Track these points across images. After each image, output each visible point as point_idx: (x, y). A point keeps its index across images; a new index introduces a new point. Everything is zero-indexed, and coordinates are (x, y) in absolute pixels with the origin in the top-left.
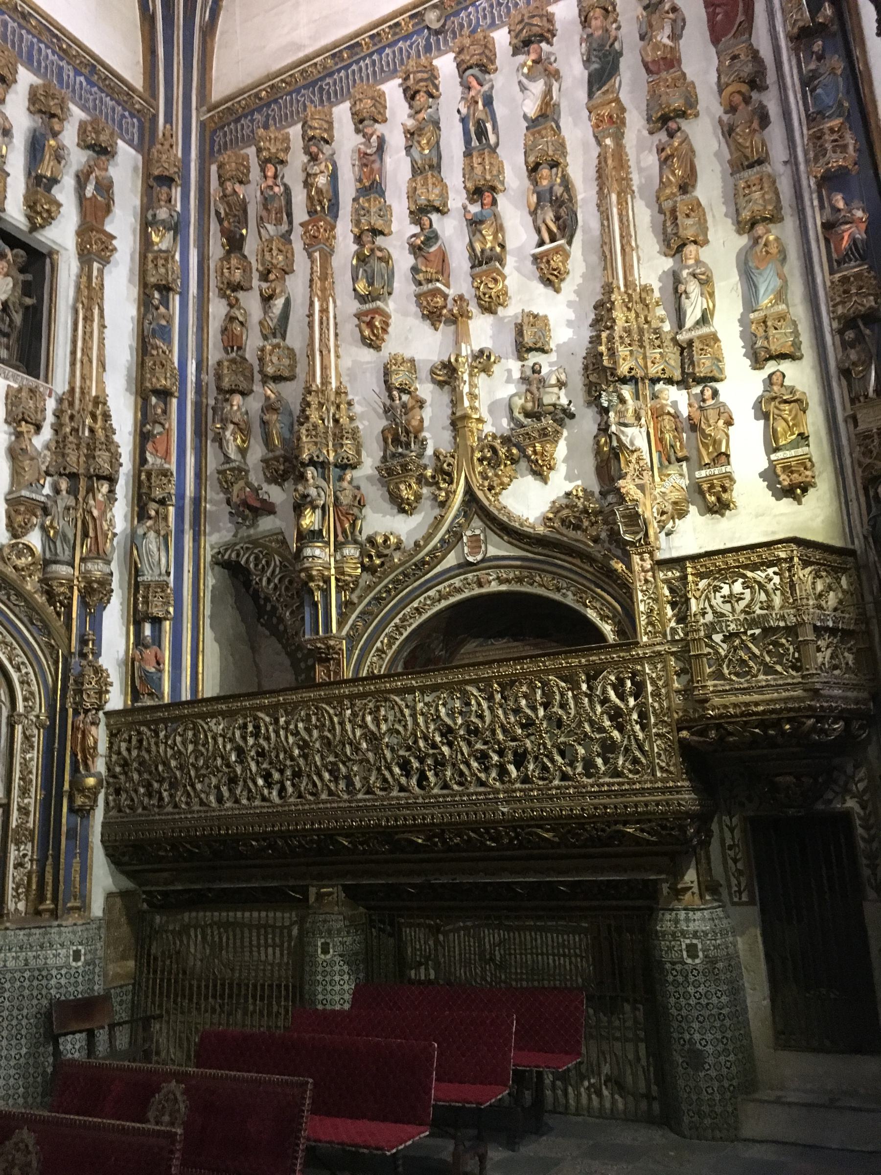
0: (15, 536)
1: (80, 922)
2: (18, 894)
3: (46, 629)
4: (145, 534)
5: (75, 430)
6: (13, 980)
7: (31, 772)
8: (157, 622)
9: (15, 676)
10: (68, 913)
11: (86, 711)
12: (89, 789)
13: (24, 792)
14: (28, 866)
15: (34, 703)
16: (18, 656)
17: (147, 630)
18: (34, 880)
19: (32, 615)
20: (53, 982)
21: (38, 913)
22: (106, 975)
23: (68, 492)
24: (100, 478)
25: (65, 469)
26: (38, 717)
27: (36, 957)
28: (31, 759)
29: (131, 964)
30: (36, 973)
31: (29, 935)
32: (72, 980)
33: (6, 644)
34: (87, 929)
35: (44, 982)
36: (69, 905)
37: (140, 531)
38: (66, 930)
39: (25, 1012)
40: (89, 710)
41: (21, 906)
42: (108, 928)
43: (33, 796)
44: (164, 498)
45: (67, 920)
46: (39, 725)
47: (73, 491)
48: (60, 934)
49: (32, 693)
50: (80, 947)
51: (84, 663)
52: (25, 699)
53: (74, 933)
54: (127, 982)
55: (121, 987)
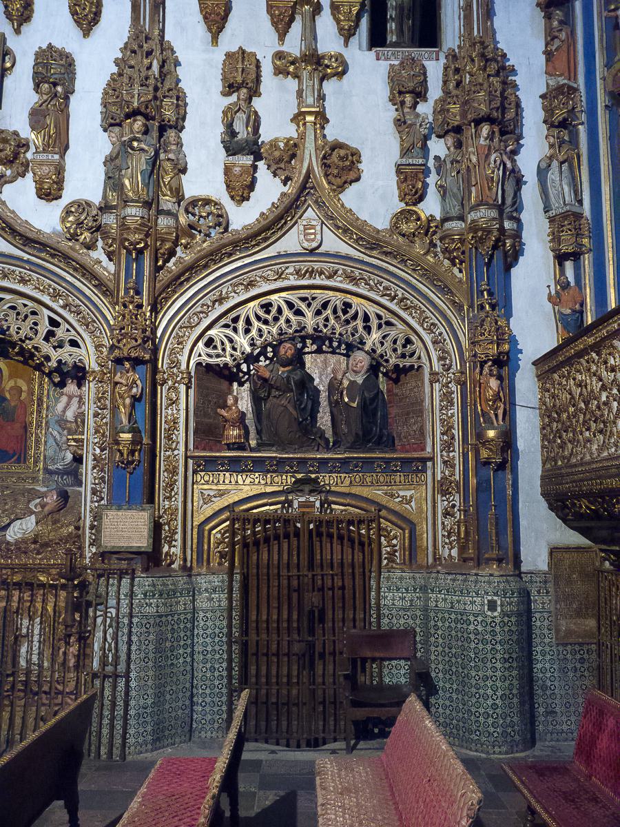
0: (407, 204)
1: (497, 573)
2: (451, 543)
3: (445, 289)
4: (550, 166)
5: (458, 84)
6: (443, 620)
7: (452, 427)
8: (576, 256)
9: (428, 338)
10: (487, 563)
11: (483, 364)
12: (492, 440)
13: (448, 446)
14: (457, 515)
15: (451, 360)
16: (427, 318)
17: (569, 266)
18: (463, 529)
19: (431, 276)
20: (472, 627)
21: (465, 560)
22: (558, 631)
23: (456, 148)
24: (478, 122)
25: (448, 124)
26: (454, 374)
27: (459, 602)
28: (453, 415)
29: (591, 623)
30: (459, 617)
31: (454, 580)
32: (489, 629)
33: (415, 307)
34: (507, 581)
35: (465, 626)
36: (486, 556)
37: (544, 165)
38: (483, 579)
39: (454, 651)
40: (486, 362)
41: (454, 552)
42: (556, 584)
43: (457, 450)
44: (565, 120)
45: (484, 569)
46: (458, 382)
47: (459, 145)
48: (476, 582)
49: (447, 352)
50: (495, 598)
51: (483, 315)
52: (441, 359)
53: (489, 583)
54: (587, 640)
55: (580, 644)
